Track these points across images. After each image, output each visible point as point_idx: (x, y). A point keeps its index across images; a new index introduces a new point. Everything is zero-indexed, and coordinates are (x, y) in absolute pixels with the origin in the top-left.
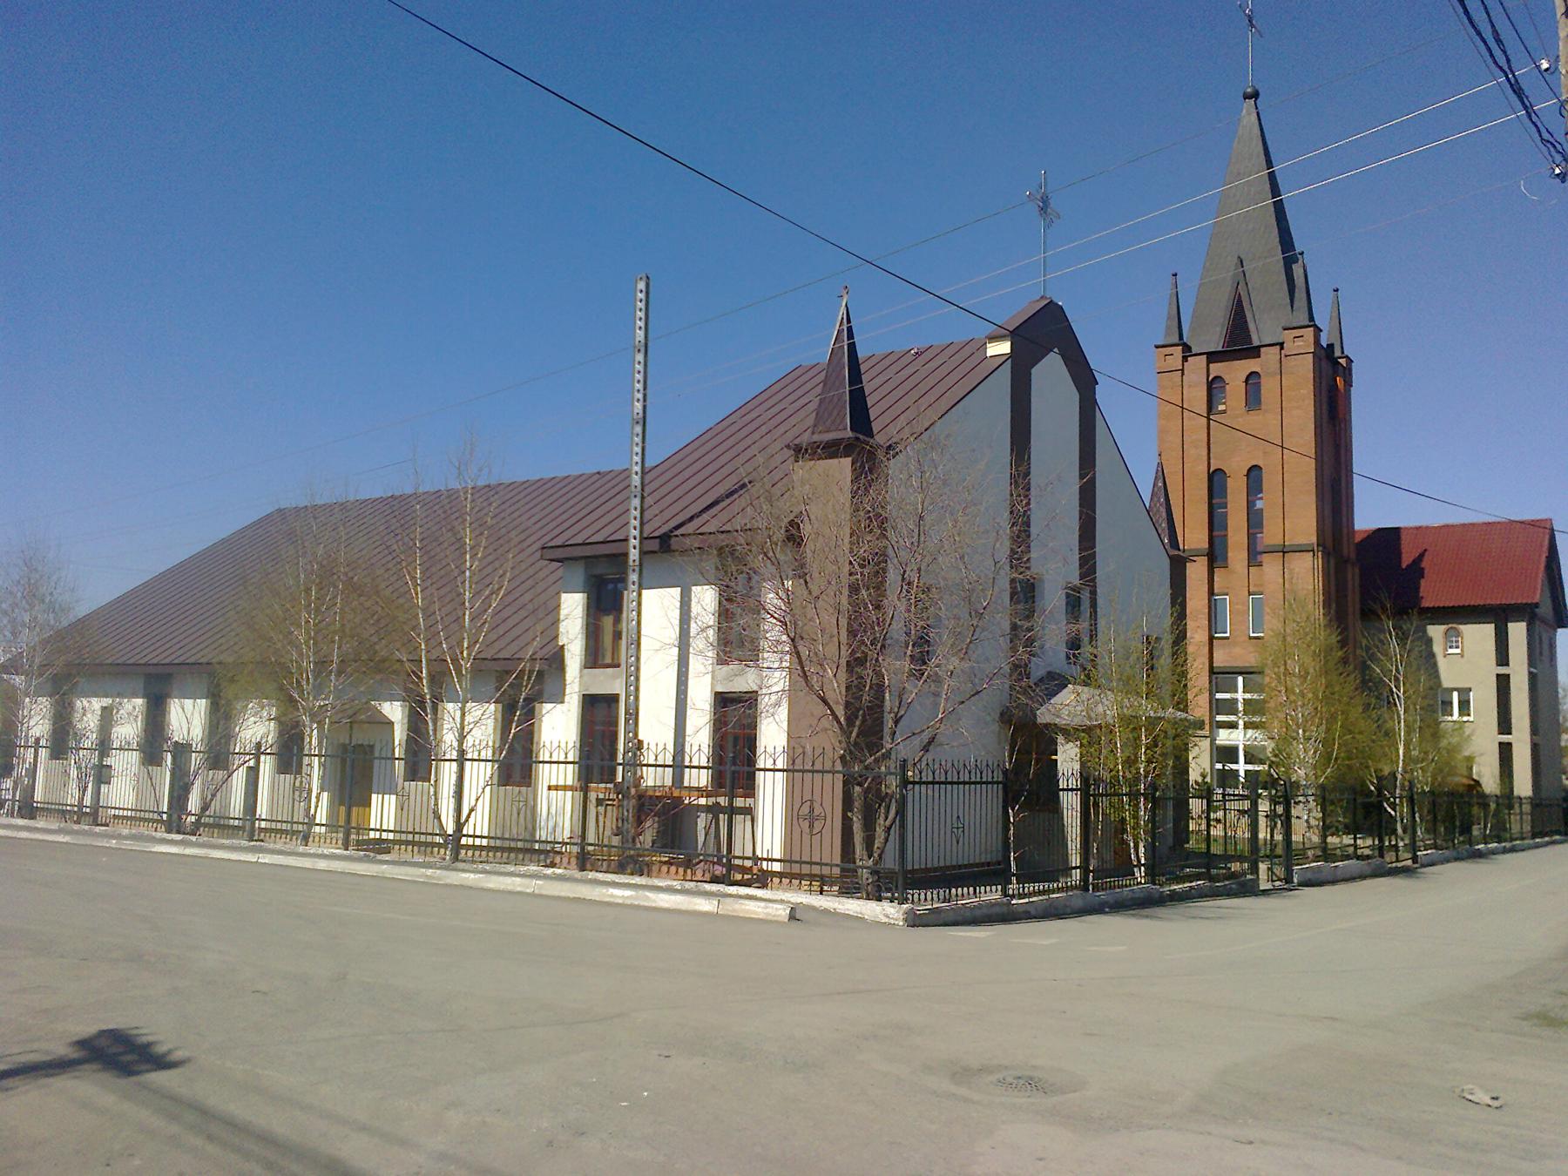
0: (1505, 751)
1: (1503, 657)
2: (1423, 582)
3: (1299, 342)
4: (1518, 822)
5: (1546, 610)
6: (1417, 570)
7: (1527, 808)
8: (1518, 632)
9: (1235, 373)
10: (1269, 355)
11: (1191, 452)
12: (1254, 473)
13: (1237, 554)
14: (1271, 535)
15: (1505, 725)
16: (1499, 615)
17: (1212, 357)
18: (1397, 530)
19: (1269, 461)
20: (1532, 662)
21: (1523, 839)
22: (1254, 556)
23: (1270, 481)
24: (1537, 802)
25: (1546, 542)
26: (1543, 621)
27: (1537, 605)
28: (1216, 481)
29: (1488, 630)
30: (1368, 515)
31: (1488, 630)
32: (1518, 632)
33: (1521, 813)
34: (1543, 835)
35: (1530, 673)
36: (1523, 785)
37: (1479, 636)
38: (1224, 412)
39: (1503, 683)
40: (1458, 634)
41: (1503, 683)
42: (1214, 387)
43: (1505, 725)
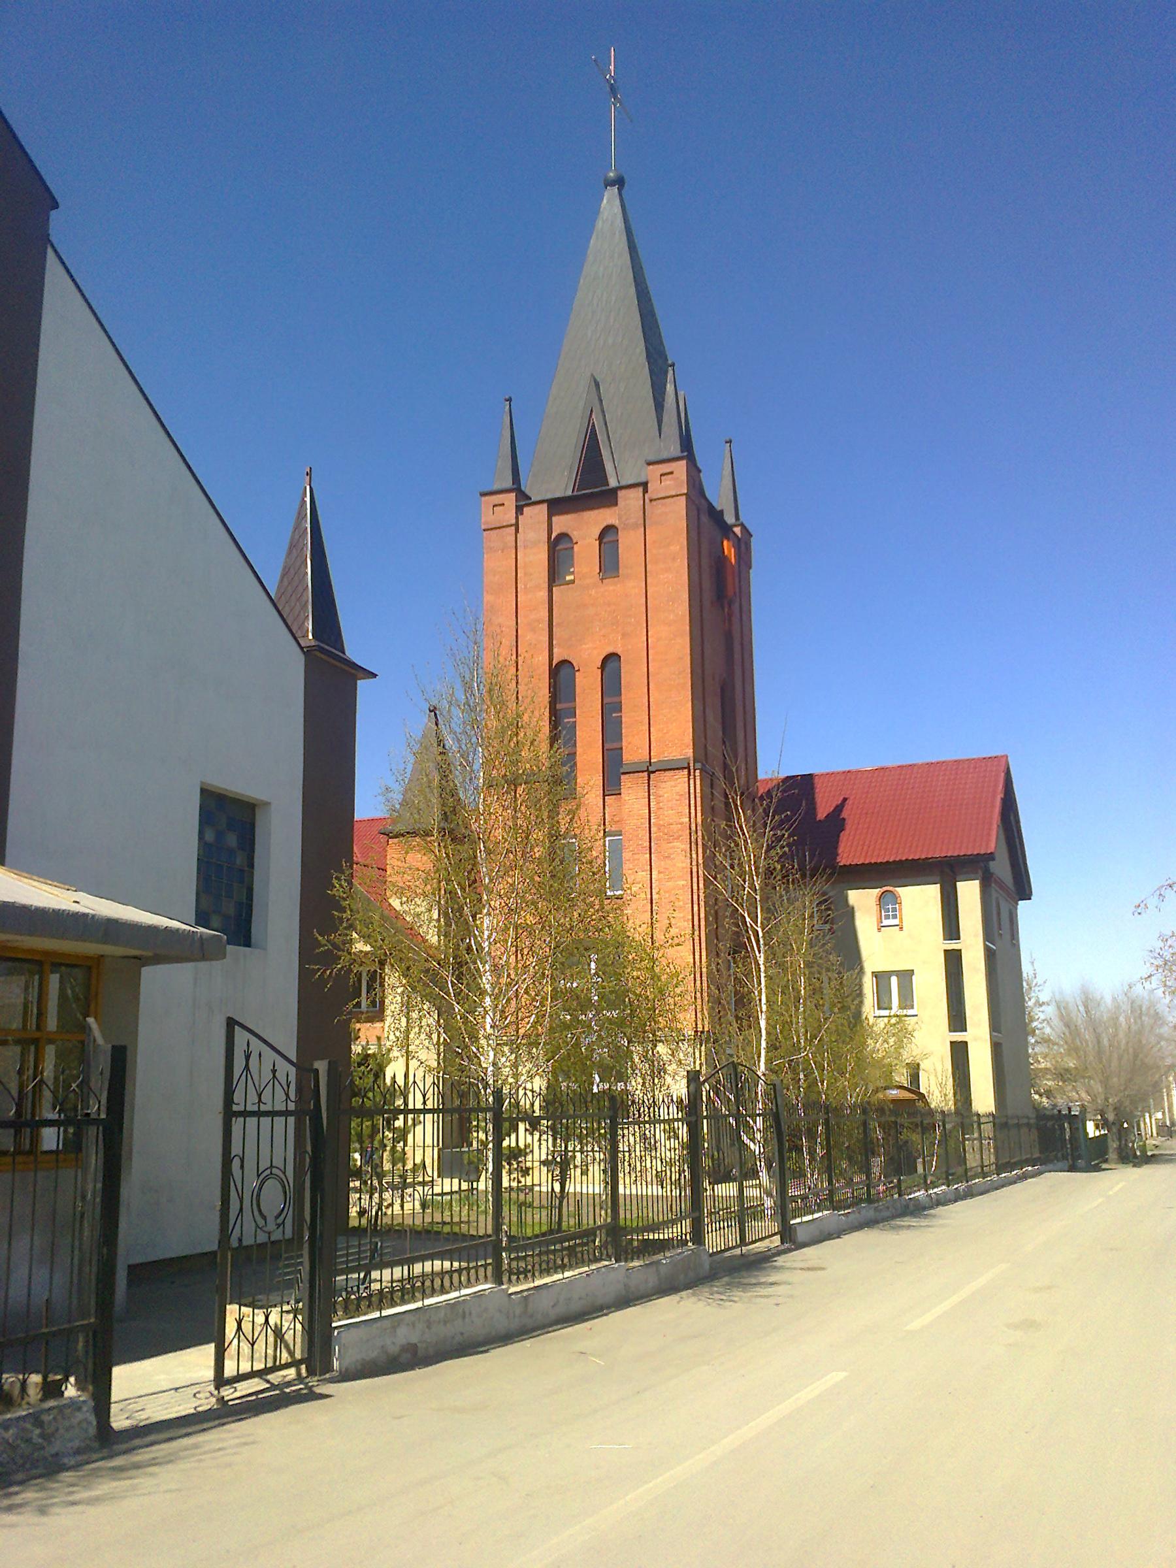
0: (959, 1052)
1: (952, 928)
2: (844, 836)
3: (667, 481)
4: (978, 1152)
5: (1001, 868)
6: (836, 821)
7: (987, 1129)
8: (969, 892)
9: (585, 528)
10: (630, 500)
11: (526, 637)
12: (611, 661)
13: (589, 778)
14: (634, 750)
15: (957, 1019)
16: (945, 872)
17: (557, 506)
18: (810, 777)
19: (631, 650)
20: (988, 935)
21: (984, 1175)
22: (611, 787)
23: (631, 675)
24: (1001, 1121)
25: (1000, 796)
26: (1001, 885)
27: (991, 857)
28: (560, 675)
29: (932, 892)
30: (775, 761)
31: (932, 892)
32: (969, 892)
33: (980, 1138)
34: (1010, 1167)
35: (987, 950)
36: (983, 1099)
37: (921, 901)
38: (573, 582)
39: (953, 961)
40: (896, 899)
41: (953, 961)
42: (559, 551)
43: (957, 1019)
